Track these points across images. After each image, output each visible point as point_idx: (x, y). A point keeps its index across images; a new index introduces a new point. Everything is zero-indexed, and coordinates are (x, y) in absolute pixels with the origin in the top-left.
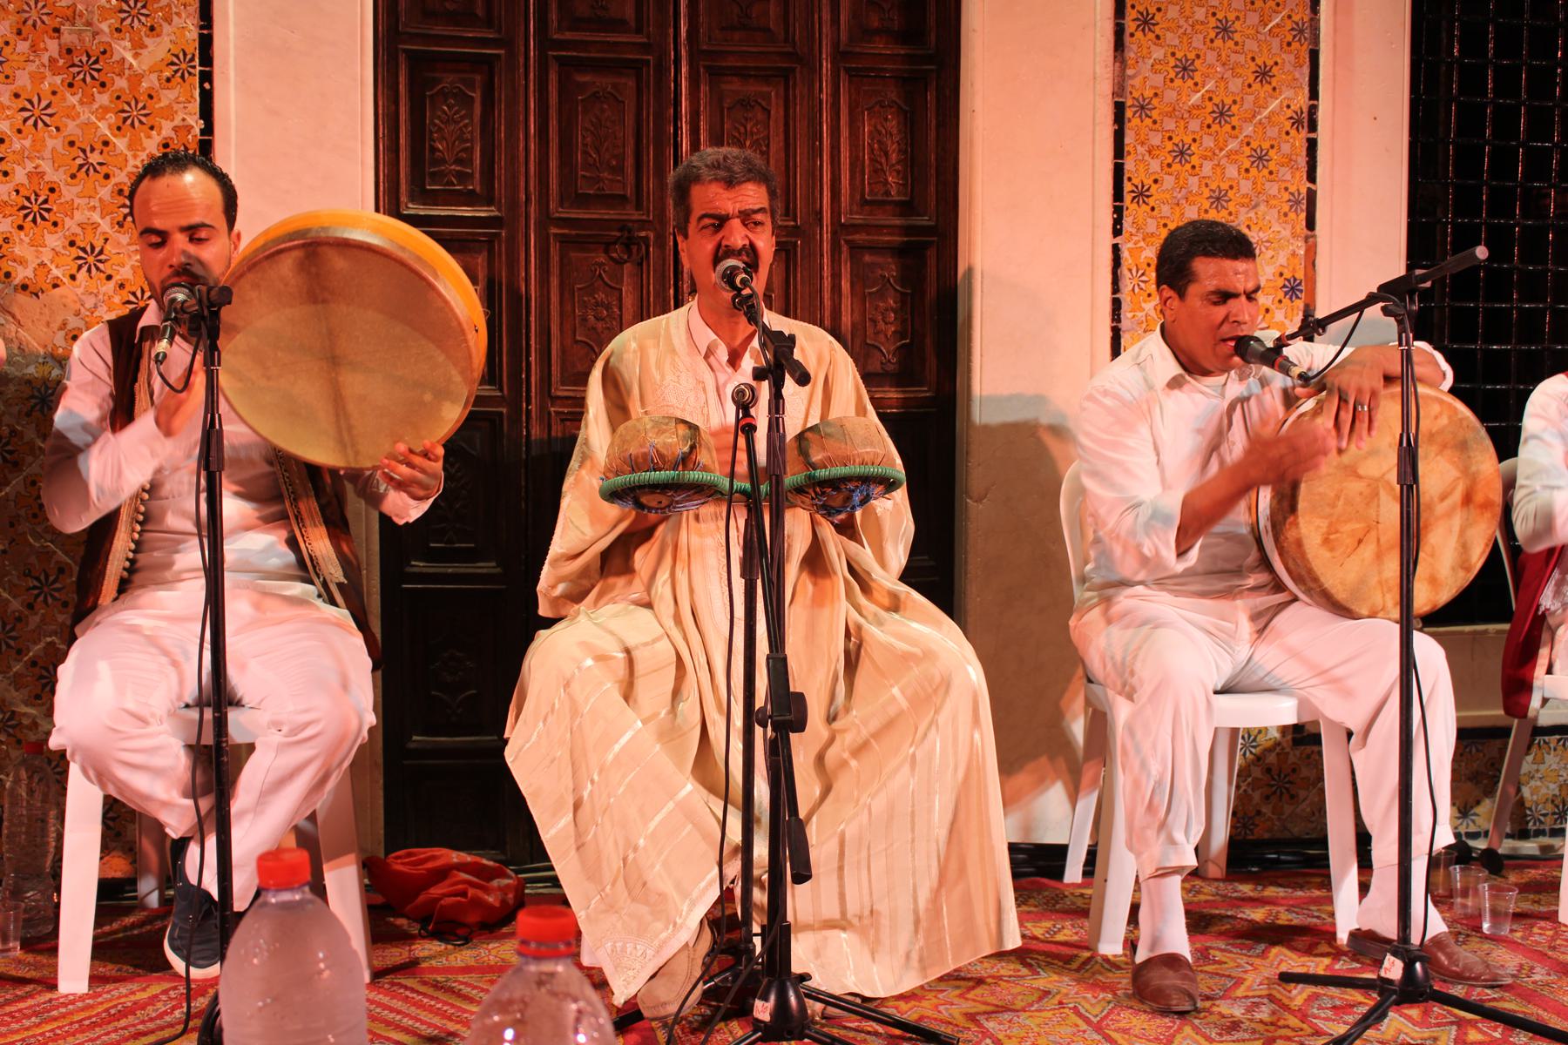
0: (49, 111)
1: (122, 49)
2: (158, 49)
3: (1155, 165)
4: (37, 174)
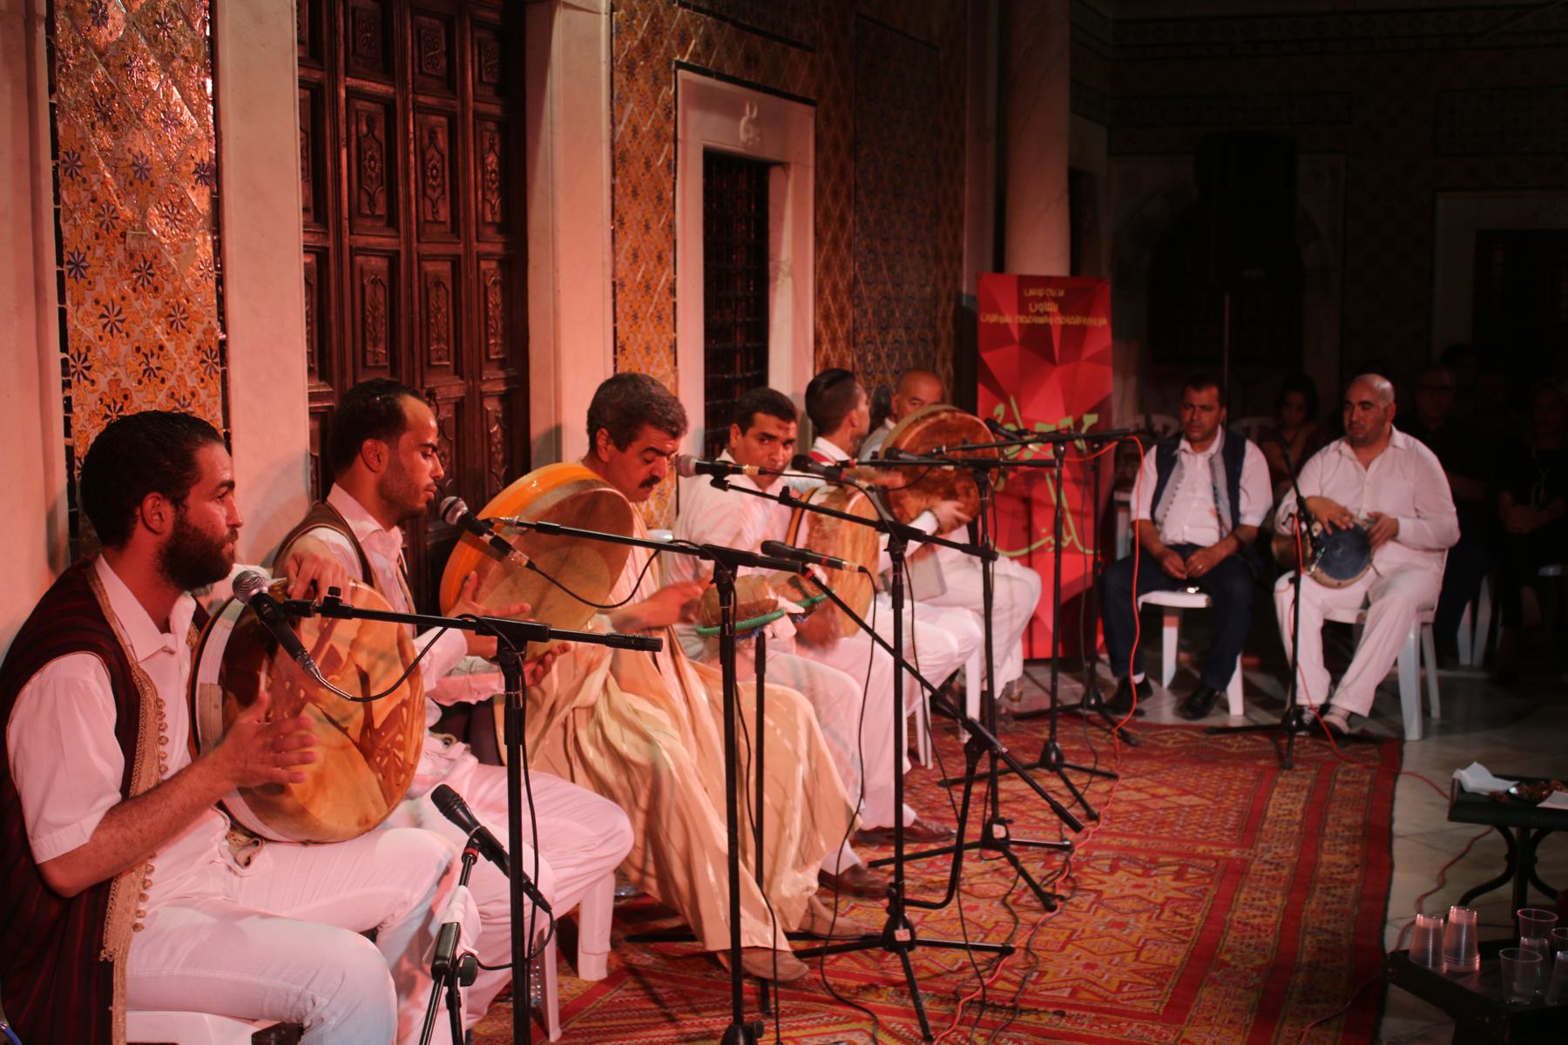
0: (121, 317)
4: (115, 382)
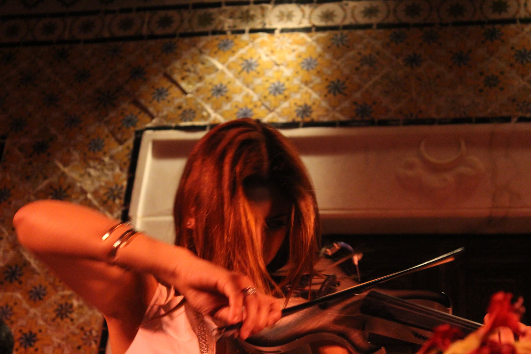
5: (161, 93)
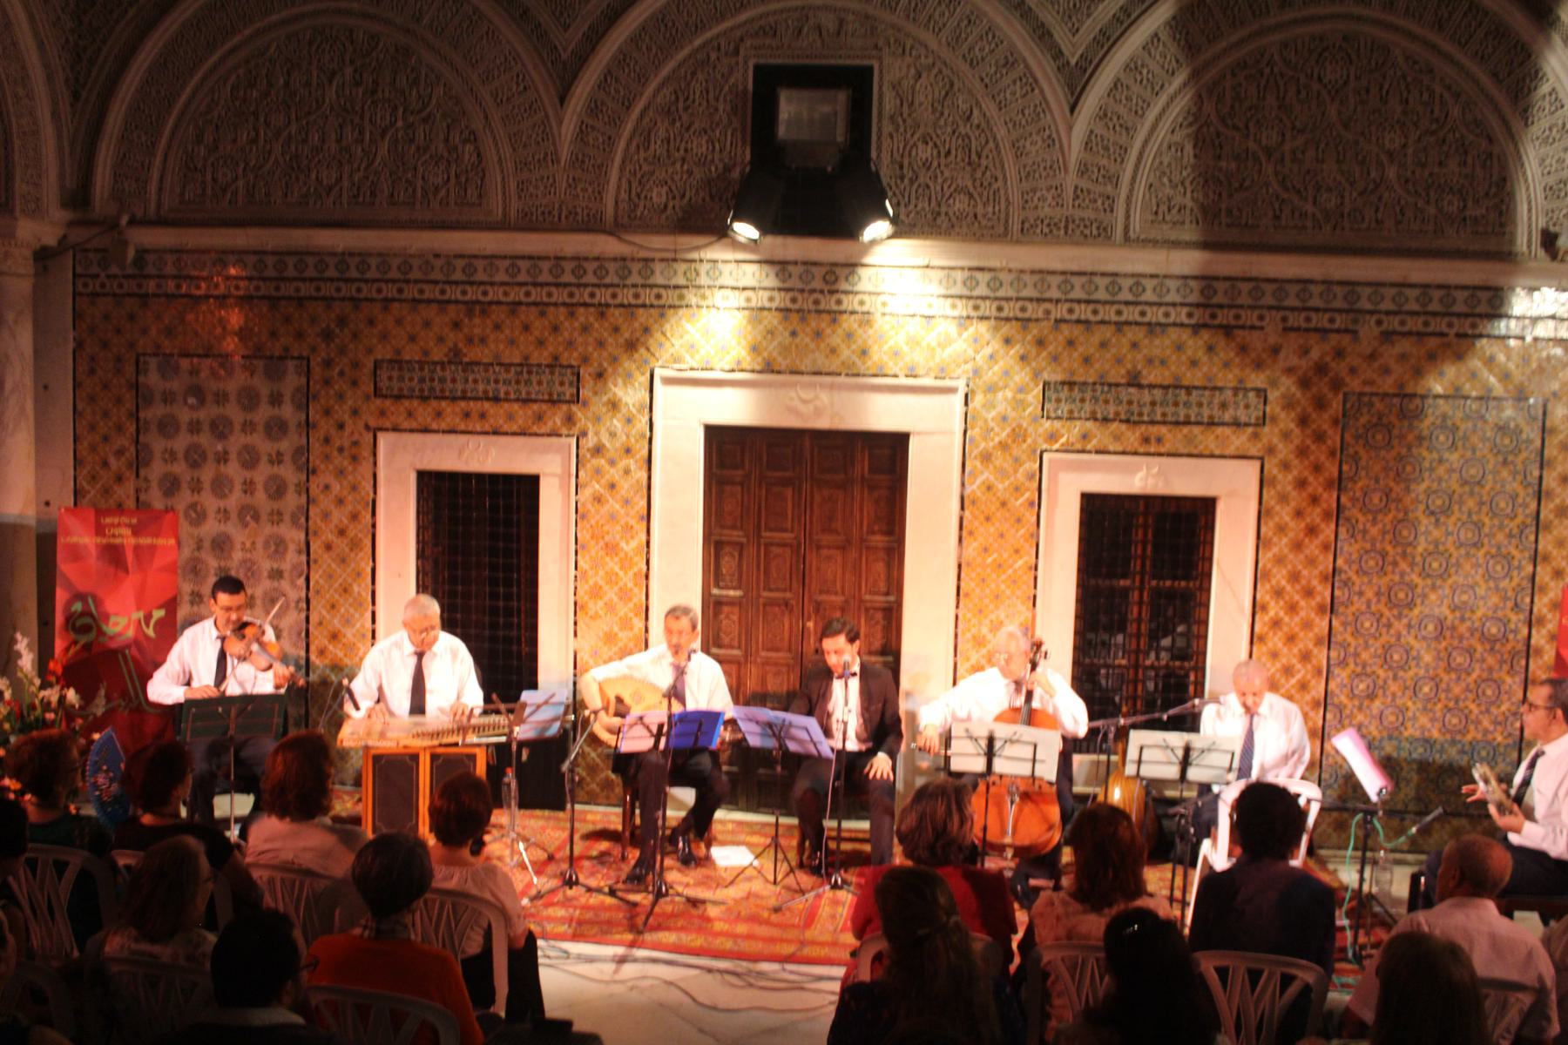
1: (623, 544)
2: (634, 544)
3: (973, 585)
5: (661, 345)
